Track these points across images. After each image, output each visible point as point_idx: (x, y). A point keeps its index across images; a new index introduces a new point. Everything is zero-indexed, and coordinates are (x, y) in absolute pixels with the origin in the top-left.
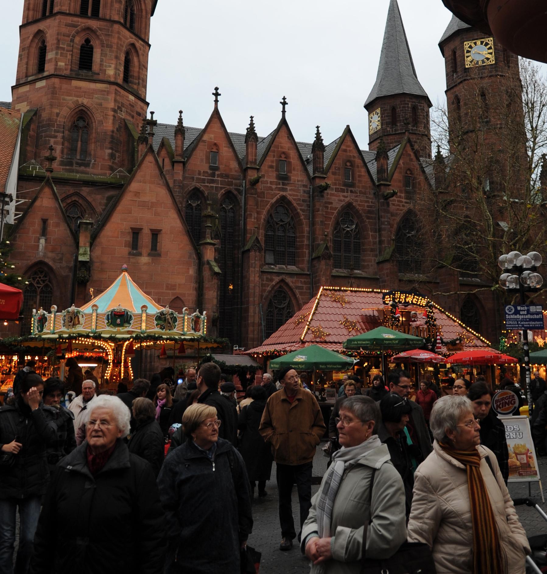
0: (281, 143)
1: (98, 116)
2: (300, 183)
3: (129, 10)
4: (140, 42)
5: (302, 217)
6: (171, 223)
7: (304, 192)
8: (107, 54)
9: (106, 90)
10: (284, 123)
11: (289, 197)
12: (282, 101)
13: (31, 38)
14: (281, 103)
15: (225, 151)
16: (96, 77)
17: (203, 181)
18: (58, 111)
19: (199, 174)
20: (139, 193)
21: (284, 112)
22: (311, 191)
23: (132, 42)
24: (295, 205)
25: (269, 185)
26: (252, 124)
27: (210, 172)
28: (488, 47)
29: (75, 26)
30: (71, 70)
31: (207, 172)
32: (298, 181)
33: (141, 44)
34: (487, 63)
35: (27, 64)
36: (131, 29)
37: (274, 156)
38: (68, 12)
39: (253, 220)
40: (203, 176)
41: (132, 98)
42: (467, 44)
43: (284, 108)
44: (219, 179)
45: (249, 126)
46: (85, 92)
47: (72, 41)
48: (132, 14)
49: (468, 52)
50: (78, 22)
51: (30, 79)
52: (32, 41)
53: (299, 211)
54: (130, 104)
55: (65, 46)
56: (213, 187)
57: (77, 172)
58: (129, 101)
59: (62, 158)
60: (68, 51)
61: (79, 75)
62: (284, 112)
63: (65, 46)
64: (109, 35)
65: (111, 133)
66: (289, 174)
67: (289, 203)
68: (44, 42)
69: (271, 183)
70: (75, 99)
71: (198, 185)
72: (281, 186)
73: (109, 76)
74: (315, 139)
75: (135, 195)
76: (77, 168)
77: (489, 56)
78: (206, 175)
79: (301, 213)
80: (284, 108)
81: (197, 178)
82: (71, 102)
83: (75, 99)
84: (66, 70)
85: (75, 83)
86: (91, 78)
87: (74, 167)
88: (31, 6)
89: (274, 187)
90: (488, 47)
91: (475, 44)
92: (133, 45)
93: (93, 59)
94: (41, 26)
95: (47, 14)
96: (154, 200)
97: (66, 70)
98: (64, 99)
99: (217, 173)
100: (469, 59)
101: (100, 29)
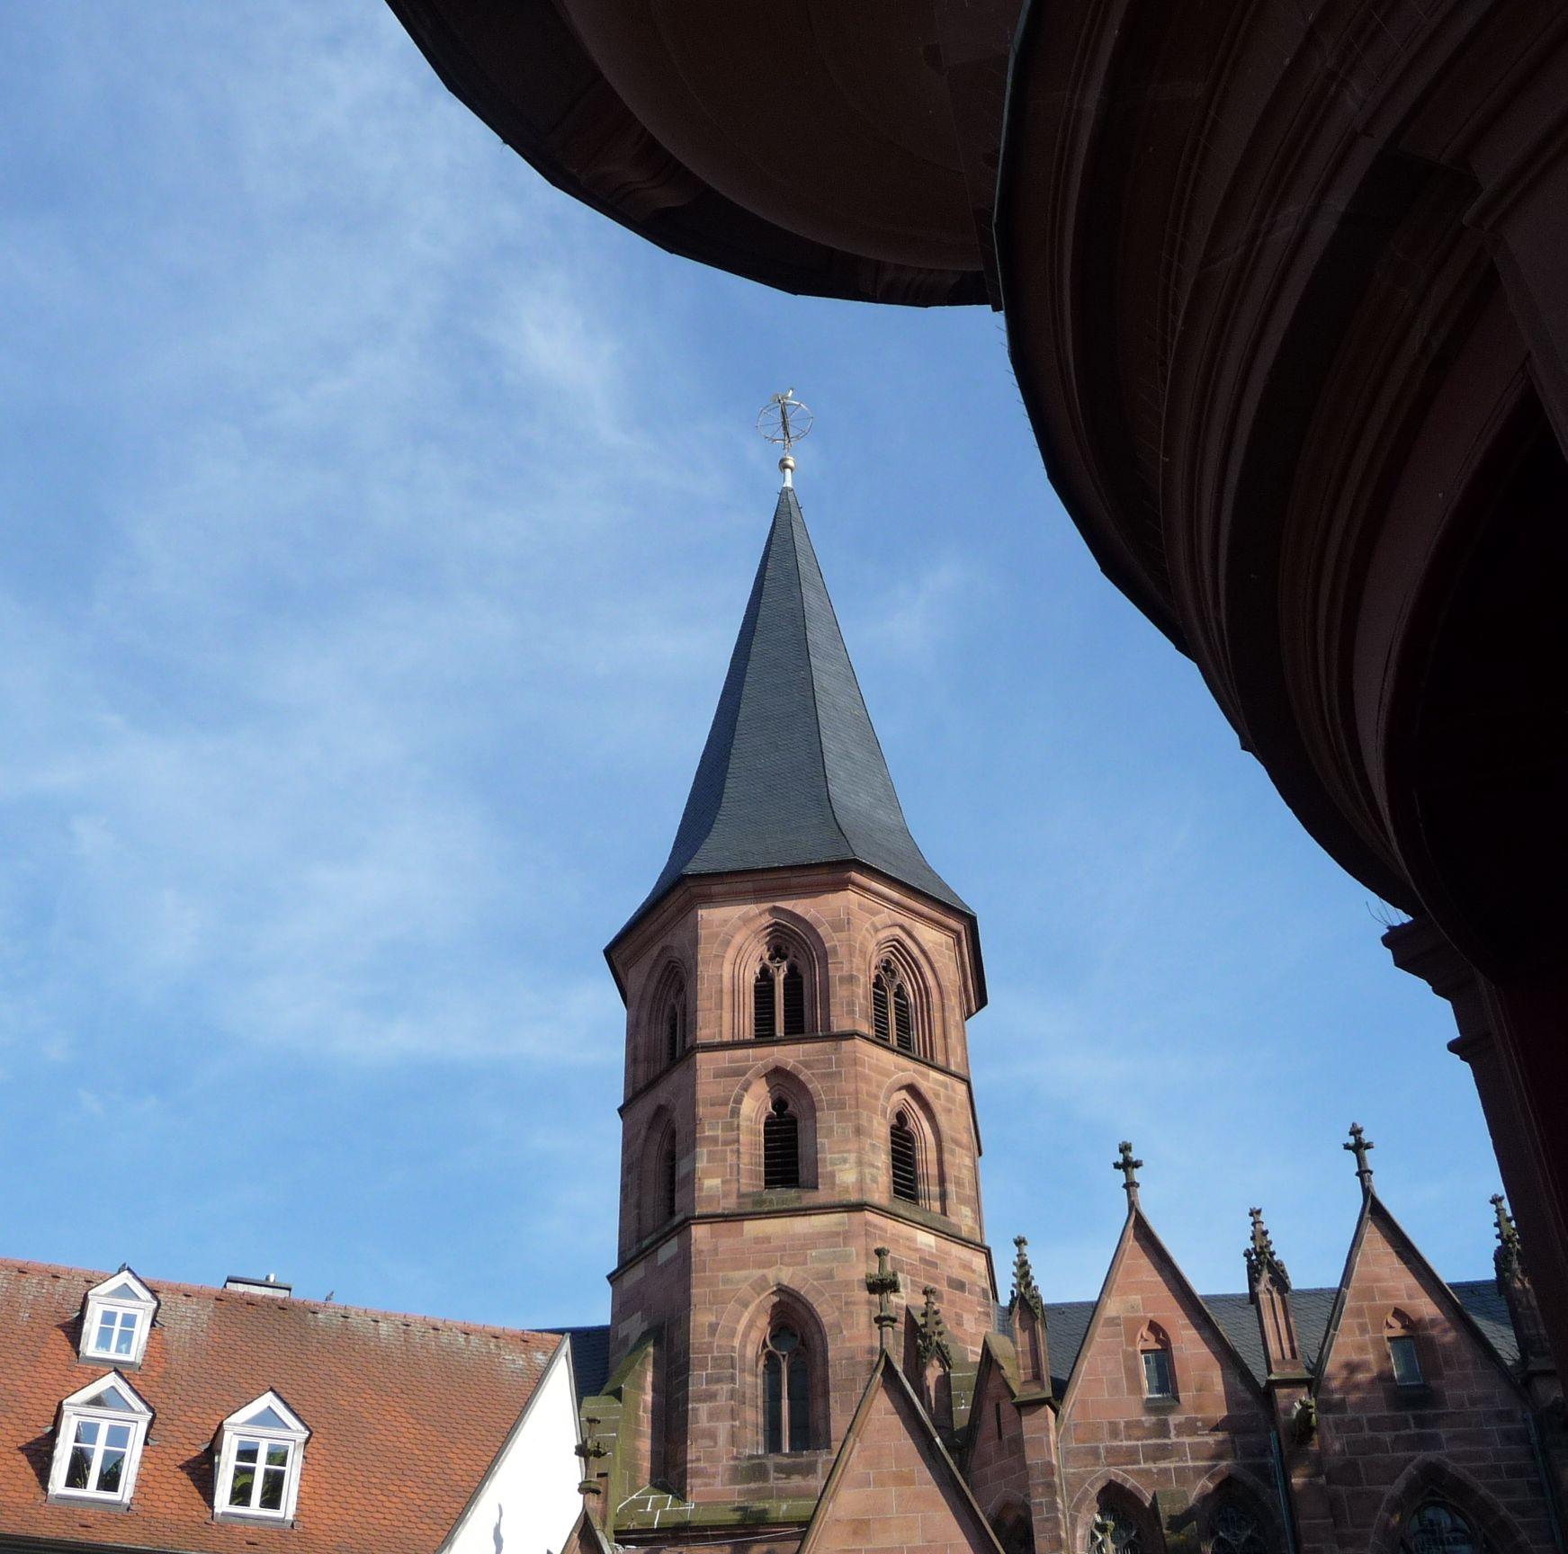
1: (826, 1312)
3: (891, 999)
4: (934, 1074)
5: (1524, 1536)
7: (1507, 1437)
8: (831, 1128)
9: (841, 1229)
10: (1375, 1211)
11: (1451, 1466)
12: (1351, 1140)
13: (643, 1132)
14: (1347, 1147)
15: (1189, 1346)
16: (810, 1198)
17: (1131, 1455)
18: (713, 1319)
19: (1114, 1433)
21: (1363, 1173)
23: (908, 1081)
24: (1483, 1491)
25: (1367, 1434)
26: (1260, 1235)
27: (1149, 1420)
30: (741, 1196)
31: (1138, 1424)
32: (1474, 1401)
33: (937, 1081)
35: (639, 1206)
36: (905, 1047)
37: (1363, 1329)
38: (717, 1040)
40: (1129, 1438)
41: (926, 1239)
43: (1361, 1160)
44: (1186, 1440)
45: (1251, 1245)
47: (735, 1113)
48: (902, 1009)
51: (646, 1243)
52: (646, 1140)
53: (1503, 1512)
54: (923, 1260)
56: (1167, 1470)
57: (782, 1495)
58: (917, 1250)
59: (736, 1458)
60: (726, 1143)
61: (762, 1202)
62: (1363, 1173)
65: (867, 1357)
66: (1433, 1383)
67: (1460, 1489)
69: (1374, 1424)
70: (759, 1272)
71: (1117, 1473)
72: (1413, 1430)
73: (846, 1190)
74: (1499, 1243)
75: (855, 1533)
76: (781, 1484)
78: (1138, 1433)
80: (1361, 1160)
81: (1109, 1450)
82: (745, 1286)
83: (758, 1273)
85: (752, 1228)
86: (797, 1205)
87: (772, 1483)
88: (641, 1053)
89: (1387, 1437)
92: (912, 1089)
94: (662, 1094)
96: (918, 1542)
97: (725, 1196)
98: (726, 1281)
99: (1174, 1419)
101: (807, 1065)
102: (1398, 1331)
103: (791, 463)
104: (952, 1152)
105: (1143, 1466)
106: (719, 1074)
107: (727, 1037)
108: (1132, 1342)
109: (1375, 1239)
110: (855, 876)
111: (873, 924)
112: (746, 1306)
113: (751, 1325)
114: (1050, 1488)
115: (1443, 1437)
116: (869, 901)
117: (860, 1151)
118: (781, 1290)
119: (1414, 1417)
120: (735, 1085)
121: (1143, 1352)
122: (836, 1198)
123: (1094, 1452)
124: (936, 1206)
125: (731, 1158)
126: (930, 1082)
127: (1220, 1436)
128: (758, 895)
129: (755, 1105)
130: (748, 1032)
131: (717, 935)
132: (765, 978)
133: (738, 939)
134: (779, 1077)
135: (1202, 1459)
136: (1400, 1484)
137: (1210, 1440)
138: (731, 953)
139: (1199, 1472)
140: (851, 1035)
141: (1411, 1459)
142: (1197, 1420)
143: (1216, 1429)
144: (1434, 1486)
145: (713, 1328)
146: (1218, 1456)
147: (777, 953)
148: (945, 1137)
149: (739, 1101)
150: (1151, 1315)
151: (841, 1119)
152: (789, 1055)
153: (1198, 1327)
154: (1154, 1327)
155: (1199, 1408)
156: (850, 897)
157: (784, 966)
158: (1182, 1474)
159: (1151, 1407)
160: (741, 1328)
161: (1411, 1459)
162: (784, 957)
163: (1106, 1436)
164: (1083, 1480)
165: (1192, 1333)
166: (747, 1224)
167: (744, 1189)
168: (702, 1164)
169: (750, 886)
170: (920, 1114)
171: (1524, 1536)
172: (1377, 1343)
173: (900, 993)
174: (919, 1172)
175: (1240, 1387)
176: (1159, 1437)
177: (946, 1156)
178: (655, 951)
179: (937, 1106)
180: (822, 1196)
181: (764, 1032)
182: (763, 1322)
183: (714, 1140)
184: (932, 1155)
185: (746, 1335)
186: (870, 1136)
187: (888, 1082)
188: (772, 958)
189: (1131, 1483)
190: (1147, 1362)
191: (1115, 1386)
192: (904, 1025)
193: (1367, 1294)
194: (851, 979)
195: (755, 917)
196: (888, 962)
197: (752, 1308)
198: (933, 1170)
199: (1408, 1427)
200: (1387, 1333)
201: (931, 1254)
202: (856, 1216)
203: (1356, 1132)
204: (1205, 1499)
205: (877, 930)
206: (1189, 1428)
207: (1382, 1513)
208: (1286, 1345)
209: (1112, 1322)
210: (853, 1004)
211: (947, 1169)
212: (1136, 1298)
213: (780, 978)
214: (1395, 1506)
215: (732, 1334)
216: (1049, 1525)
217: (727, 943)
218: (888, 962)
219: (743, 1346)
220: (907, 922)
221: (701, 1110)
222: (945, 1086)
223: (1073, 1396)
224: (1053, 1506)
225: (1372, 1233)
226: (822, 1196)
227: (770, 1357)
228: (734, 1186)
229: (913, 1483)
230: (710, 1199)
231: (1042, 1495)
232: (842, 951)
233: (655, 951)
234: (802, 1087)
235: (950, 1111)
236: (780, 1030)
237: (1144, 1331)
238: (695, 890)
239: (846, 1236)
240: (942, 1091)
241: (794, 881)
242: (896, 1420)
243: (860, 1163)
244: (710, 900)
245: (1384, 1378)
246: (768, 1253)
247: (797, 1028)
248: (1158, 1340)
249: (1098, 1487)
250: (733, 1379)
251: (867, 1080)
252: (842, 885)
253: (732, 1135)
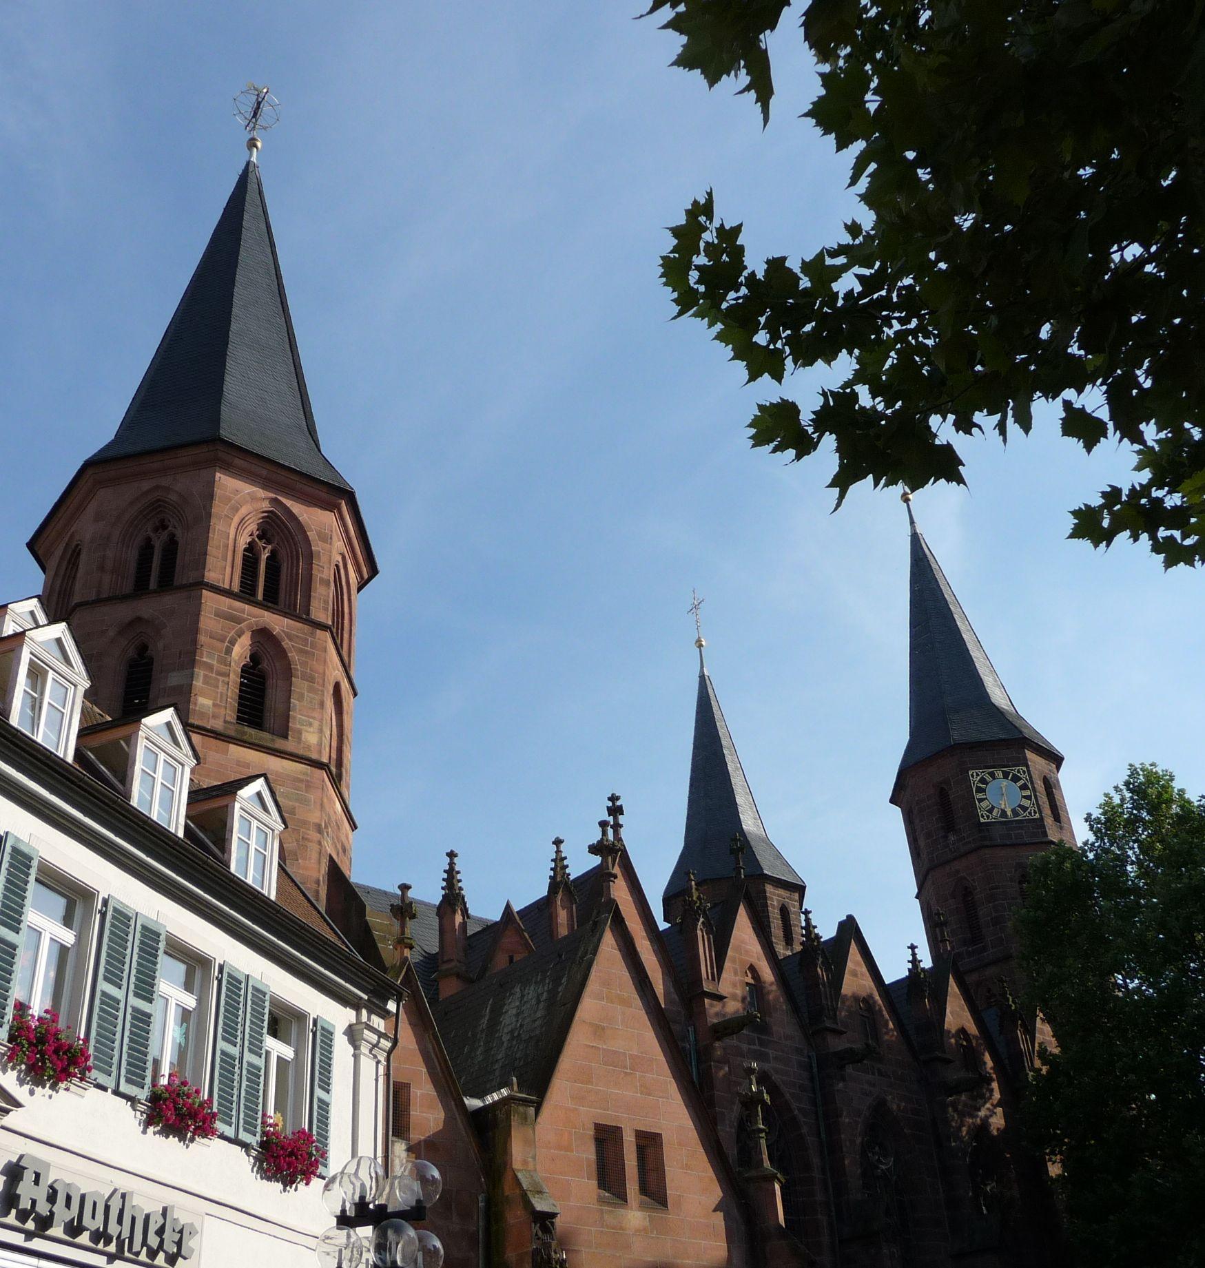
0: (743, 942)
5: (805, 1130)
6: (673, 1118)
8: (303, 695)
13: (111, 633)
16: (279, 744)
20: (603, 1028)
22: (814, 1065)
24: (788, 1096)
28: (1020, 783)
29: (238, 620)
34: (1023, 815)
37: (736, 974)
42: (975, 776)
47: (229, 651)
49: (980, 790)
50: (243, 611)
55: (215, 663)
63: (215, 663)
64: (307, 652)
68: (143, 649)
72: (757, 1047)
73: (309, 747)
77: (1026, 803)
79: (801, 1119)
84: (214, 717)
90: (1020, 783)
91: (992, 775)
93: (268, 702)
94: (147, 608)
95: (153, 584)
100: (984, 804)
101: (290, 637)
102: (750, 980)
106: (219, 614)
122: (301, 752)
128: (266, 483)
129: (241, 650)
130: (236, 588)
132: (251, 548)
133: (243, 511)
134: (263, 636)
140: (323, 627)
147: (264, 534)
149: (233, 642)
151: (311, 690)
152: (278, 623)
162: (268, 542)
166: (231, 746)
167: (228, 718)
168: (198, 683)
169: (264, 472)
178: (146, 485)
180: (290, 745)
181: (246, 592)
183: (210, 667)
188: (260, 537)
213: (265, 555)
221: (202, 638)
228: (222, 711)
232: (324, 558)
233: (146, 485)
234: (283, 653)
236: (260, 597)
241: (299, 486)
244: (228, 468)
247: (272, 601)
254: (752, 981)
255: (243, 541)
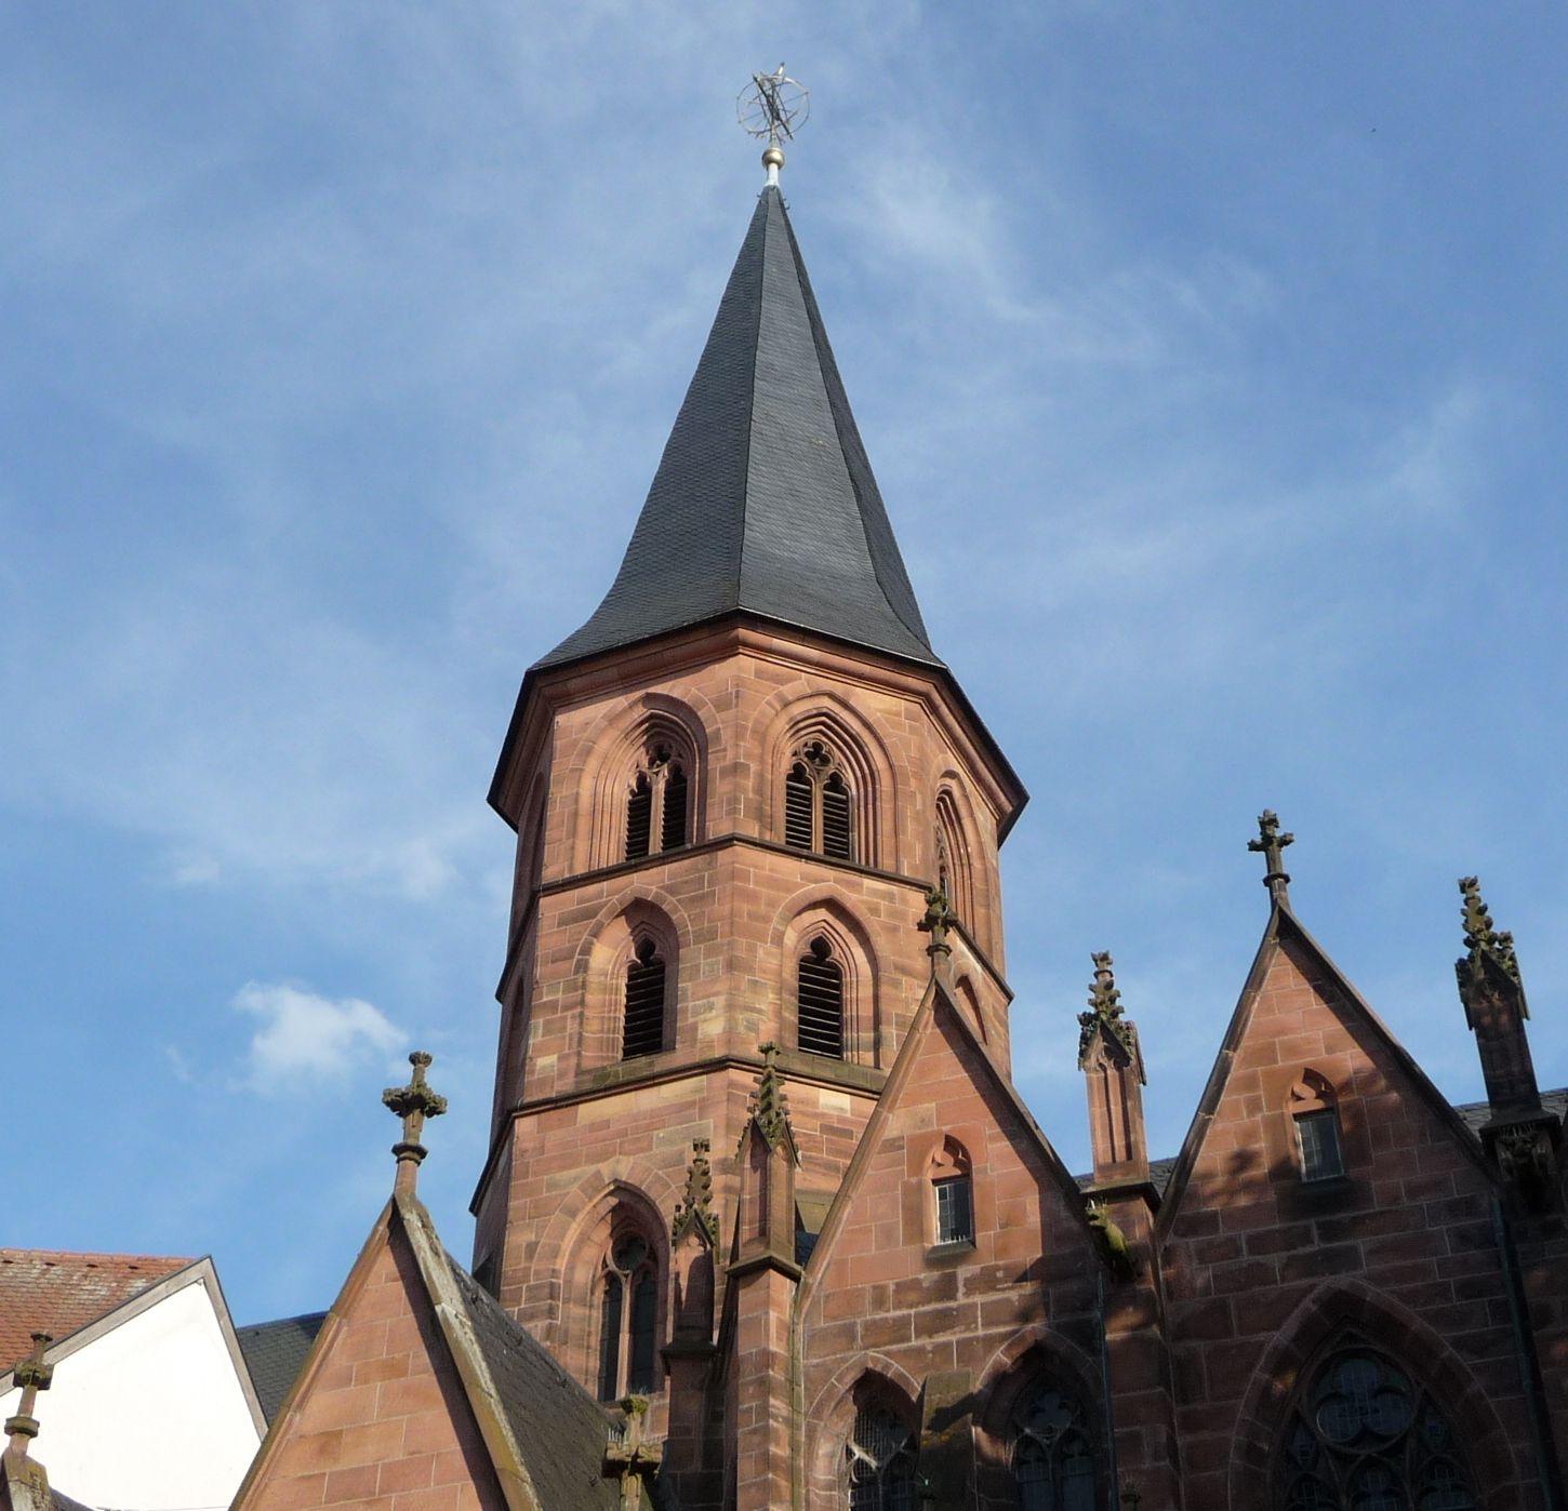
2: (1424, 1201)
4: (868, 883)
5: (1478, 1385)
7: (1463, 1238)
9: (697, 1097)
10: (1286, 932)
11: (1372, 1292)
15: (997, 1163)
17: (898, 1330)
18: (533, 1238)
19: (879, 1302)
23: (824, 895)
24: (1418, 1324)
25: (1246, 1258)
27: (928, 1277)
29: (589, 914)
30: (579, 1072)
32: (1413, 1192)
33: (875, 892)
36: (838, 853)
39: (1147, 1465)
40: (898, 1306)
44: (978, 1299)
46: (623, 1133)
47: (583, 967)
53: (1449, 1351)
54: (827, 1129)
55: (560, 996)
56: (948, 1345)
58: (816, 1116)
60: (566, 1008)
63: (560, 996)
64: (702, 897)
67: (1386, 1325)
69: (1258, 1244)
72: (1317, 1246)
73: (710, 1045)
78: (912, 1297)
81: (871, 1327)
82: (574, 1188)
83: (590, 1169)
85: (588, 1111)
89: (1275, 1260)
92: (832, 905)
96: (400, 1456)
97: (562, 1075)
98: (551, 1186)
99: (964, 1272)
101: (671, 890)
103: (776, 155)
104: (896, 984)
105: (914, 1343)
107: (580, 869)
108: (917, 1169)
109: (1284, 973)
110: (743, 633)
111: (780, 697)
112: (573, 1214)
113: (583, 1239)
114: (765, 1387)
115: (1362, 1250)
116: (771, 667)
117: (732, 993)
118: (621, 1188)
119: (1320, 1226)
120: (583, 930)
121: (936, 1182)
123: (848, 1333)
124: (868, 1058)
125: (572, 1027)
126: (861, 893)
127: (1028, 1288)
128: (626, 683)
131: (575, 744)
132: (643, 788)
133: (603, 745)
135: (1005, 1323)
136: (1291, 1326)
137: (1013, 1295)
138: (593, 764)
139: (990, 1343)
140: (727, 842)
141: (1312, 1287)
142: (997, 1268)
143: (1023, 1278)
144: (1345, 1330)
145: (531, 1249)
146: (1024, 1316)
147: (658, 755)
148: (882, 964)
149: (587, 950)
150: (946, 1129)
151: (709, 953)
152: (647, 882)
153: (1011, 1137)
154: (952, 1145)
155: (1002, 1251)
156: (743, 665)
157: (665, 770)
158: (967, 1348)
159: (936, 1259)
160: (568, 1244)
161: (1312, 1287)
162: (664, 759)
163: (868, 1306)
164: (830, 1372)
165: (1004, 1146)
167: (587, 1064)
169: (612, 673)
170: (851, 939)
171: (1478, 1385)
172: (1276, 1125)
173: (835, 783)
174: (846, 1015)
175: (1064, 1214)
176: (940, 1299)
177: (884, 989)
179: (872, 924)
180: (680, 1056)
182: (603, 1234)
183: (553, 1006)
184: (866, 992)
185: (574, 1255)
186: (750, 970)
187: (788, 898)
188: (652, 763)
189: (895, 1369)
190: (942, 1195)
191: (888, 1234)
192: (838, 825)
193: (1266, 1054)
194: (736, 769)
195: (625, 711)
196: (817, 746)
197: (580, 1217)
198: (867, 1011)
199: (1309, 1241)
200: (1294, 1108)
201: (841, 1120)
202: (719, 1078)
203: (1268, 822)
204: (999, 1379)
205: (786, 704)
206: (987, 1281)
207: (1259, 1374)
208: (1119, 1142)
209: (893, 1145)
210: (736, 800)
211: (883, 1007)
212: (929, 1107)
213: (659, 787)
214: (1282, 1362)
215: (555, 1253)
216: (756, 1439)
217: (588, 752)
218: (817, 746)
219: (571, 1267)
220: (838, 688)
222: (890, 897)
223: (824, 1260)
224: (765, 1412)
225: (1282, 967)
226: (680, 1056)
227: (612, 1280)
228: (573, 1061)
229: (404, 1373)
230: (543, 1082)
231: (753, 1397)
232: (727, 736)
235: (895, 929)
237: (938, 1152)
238: (547, 691)
239: (703, 1106)
240: (883, 904)
241: (668, 654)
242: (399, 1288)
243: (730, 1007)
245: (1283, 1169)
246: (609, 1140)
248: (957, 1163)
249: (850, 1379)
250: (551, 1312)
251: (752, 897)
252: (729, 650)
253: (576, 996)
254: (1319, 1104)
255: (620, 791)
